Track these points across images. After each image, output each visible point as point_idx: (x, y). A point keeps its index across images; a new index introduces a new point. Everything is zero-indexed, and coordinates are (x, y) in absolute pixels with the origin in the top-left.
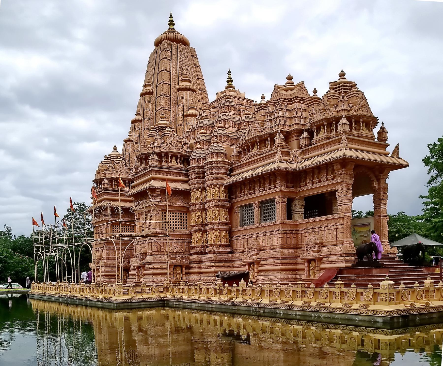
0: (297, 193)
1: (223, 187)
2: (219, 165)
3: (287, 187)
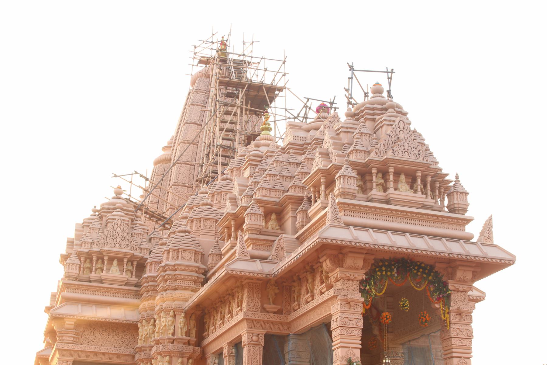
0: (289, 324)
1: (183, 315)
2: (177, 272)
3: (264, 310)
